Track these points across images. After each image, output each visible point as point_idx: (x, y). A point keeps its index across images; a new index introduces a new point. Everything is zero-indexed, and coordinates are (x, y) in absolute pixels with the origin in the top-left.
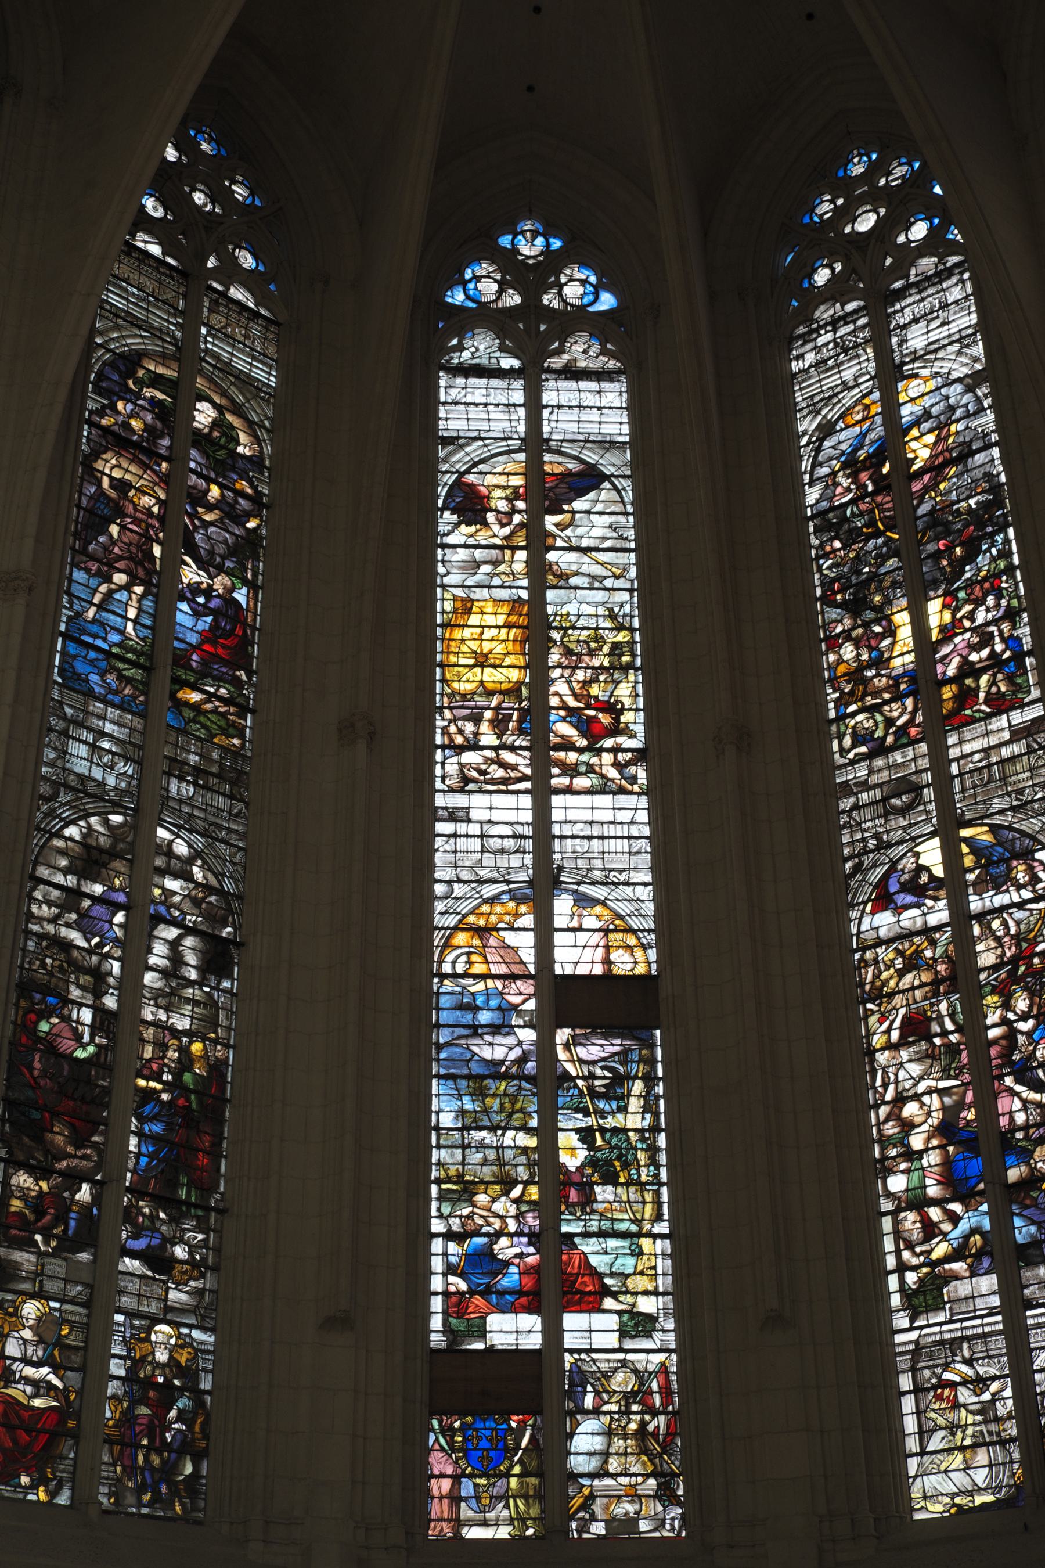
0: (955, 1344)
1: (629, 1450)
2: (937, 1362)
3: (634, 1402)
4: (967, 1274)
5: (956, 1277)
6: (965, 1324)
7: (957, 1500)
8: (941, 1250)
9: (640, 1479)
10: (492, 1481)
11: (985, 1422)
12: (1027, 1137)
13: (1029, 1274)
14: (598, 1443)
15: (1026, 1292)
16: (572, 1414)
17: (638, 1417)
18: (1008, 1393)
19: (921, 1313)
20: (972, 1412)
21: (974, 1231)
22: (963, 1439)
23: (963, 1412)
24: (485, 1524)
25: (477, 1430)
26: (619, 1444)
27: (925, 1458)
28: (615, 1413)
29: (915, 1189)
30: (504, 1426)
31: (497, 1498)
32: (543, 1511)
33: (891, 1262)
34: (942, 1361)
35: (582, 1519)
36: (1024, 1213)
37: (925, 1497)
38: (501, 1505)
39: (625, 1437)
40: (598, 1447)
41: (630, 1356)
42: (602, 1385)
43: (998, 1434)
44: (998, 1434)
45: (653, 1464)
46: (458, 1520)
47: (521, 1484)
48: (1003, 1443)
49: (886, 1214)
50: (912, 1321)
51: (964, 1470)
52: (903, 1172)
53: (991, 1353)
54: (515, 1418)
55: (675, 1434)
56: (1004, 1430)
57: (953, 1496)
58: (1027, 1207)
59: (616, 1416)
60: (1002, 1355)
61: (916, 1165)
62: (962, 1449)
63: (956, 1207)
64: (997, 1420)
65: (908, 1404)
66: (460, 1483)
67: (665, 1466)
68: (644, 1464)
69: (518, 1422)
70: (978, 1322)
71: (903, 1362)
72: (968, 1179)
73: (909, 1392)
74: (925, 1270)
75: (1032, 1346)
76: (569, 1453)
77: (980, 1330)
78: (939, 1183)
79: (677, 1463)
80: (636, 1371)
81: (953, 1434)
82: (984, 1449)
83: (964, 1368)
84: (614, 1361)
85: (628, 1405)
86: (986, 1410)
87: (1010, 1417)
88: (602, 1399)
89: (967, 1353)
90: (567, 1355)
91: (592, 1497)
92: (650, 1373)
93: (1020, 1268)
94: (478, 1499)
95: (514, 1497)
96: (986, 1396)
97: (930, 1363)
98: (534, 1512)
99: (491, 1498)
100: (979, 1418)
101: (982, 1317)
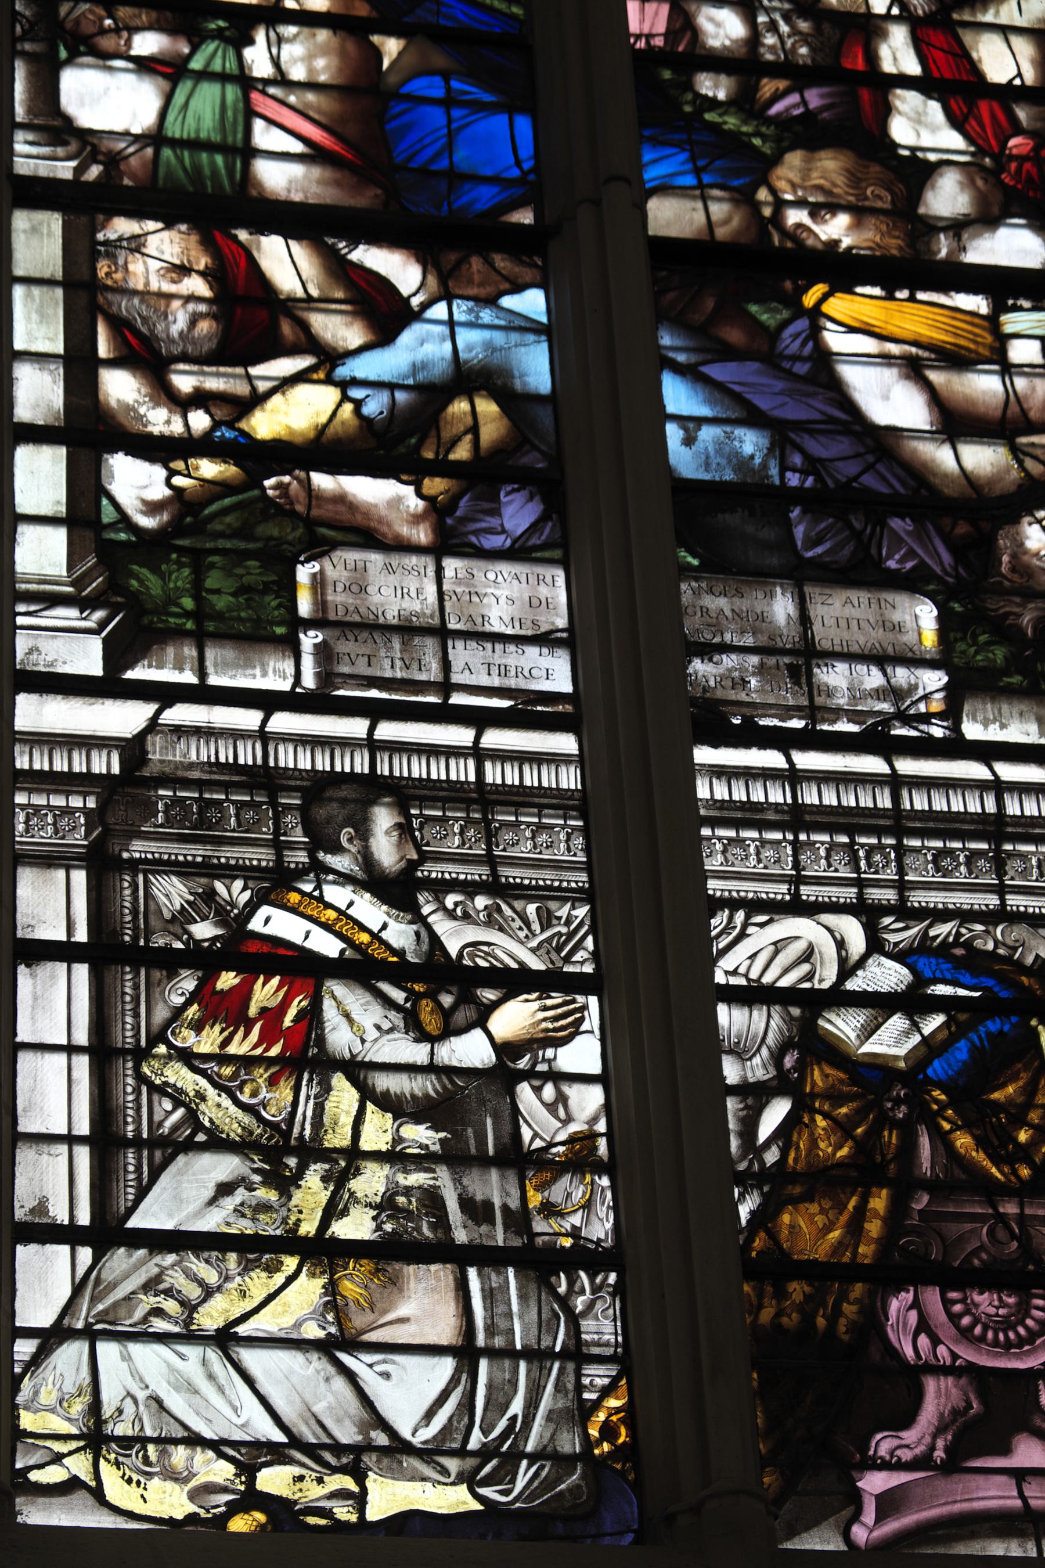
0: (332, 803)
2: (229, 854)
4: (422, 535)
5: (366, 533)
6: (387, 731)
7: (274, 1480)
8: (297, 411)
11: (454, 1157)
12: (744, 101)
13: (718, 603)
15: (698, 667)
18: (583, 1054)
19: (178, 634)
20: (394, 1106)
21: (466, 378)
22: (332, 1211)
23: (344, 1096)
27: (119, 1260)
29: (195, 144)
33: (37, 393)
34: (261, 856)
36: (716, 371)
37: (95, 1439)
43: (518, 1220)
44: (518, 1220)
48: (540, 1263)
49: (39, 194)
50: (118, 654)
51: (326, 1347)
52: (145, 65)
53: (510, 874)
56: (549, 1210)
57: (251, 1456)
58: (727, 353)
60: (563, 895)
61: (208, 55)
62: (323, 1252)
63: (400, 270)
64: (516, 1158)
65: (52, 1004)
70: (461, 736)
71: (38, 818)
72: (456, 178)
73: (64, 952)
74: (209, 469)
75: (714, 886)
77: (464, 771)
78: (315, 154)
81: (287, 1184)
82: (441, 1274)
83: (369, 911)
86: (466, 1111)
87: (580, 1157)
89: (386, 850)
93: (685, 572)
96: (471, 1050)
97: (197, 852)
100: (420, 1135)
101: (480, 720)
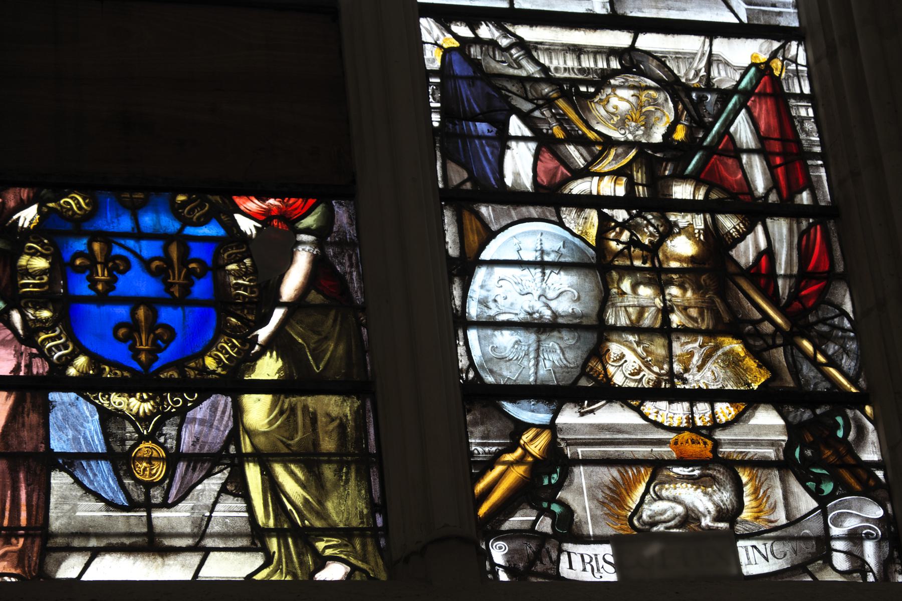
1: (676, 319)
3: (681, 176)
9: (725, 411)
10: (171, 402)
14: (564, 293)
16: (464, 201)
17: (699, 222)
24: (152, 544)
25: (108, 238)
26: (637, 298)
28: (614, 202)
30: (212, 230)
31: (194, 459)
32: (374, 508)
35: (529, 533)
38: (213, 484)
39: (659, 278)
40: (564, 306)
41: (648, 42)
42: (562, 120)
45: (765, 363)
46: (39, 528)
47: (286, 417)
54: (253, 205)
55: (830, 277)
59: (621, 215)
66: (46, 408)
67: (806, 369)
68: (732, 362)
69: (264, 218)
76: (463, 322)
79: (848, 363)
80: (673, 87)
84: (597, 51)
85: (658, 185)
88: (564, 161)
90: (429, 28)
91: (557, 461)
92: (724, 95)
94: (121, 461)
95: (264, 460)
98: (345, 506)
99: (173, 459)
